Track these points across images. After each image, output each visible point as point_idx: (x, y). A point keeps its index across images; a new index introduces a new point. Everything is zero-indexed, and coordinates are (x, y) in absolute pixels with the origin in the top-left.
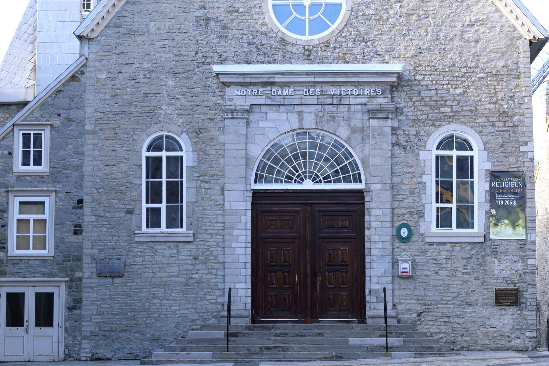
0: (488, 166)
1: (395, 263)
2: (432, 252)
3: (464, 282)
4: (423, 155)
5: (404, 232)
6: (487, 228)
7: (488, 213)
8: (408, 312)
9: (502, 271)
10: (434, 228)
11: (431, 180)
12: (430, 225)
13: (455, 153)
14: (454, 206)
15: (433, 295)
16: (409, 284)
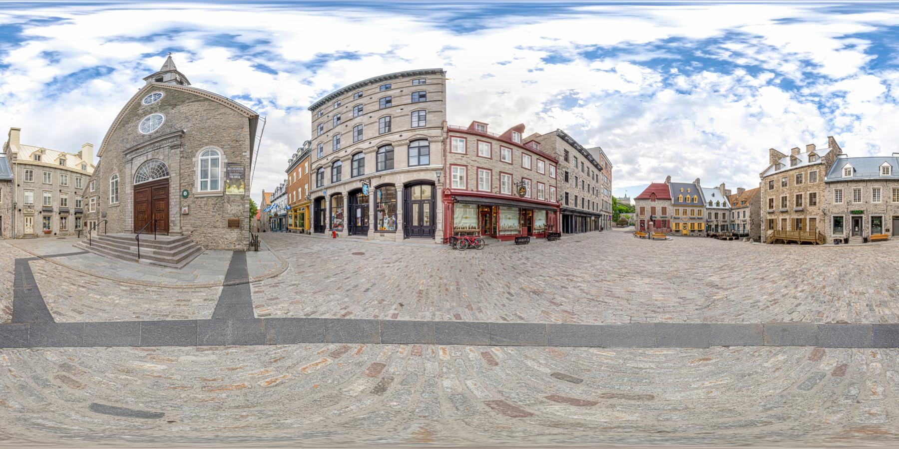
0: (226, 161)
1: (181, 209)
2: (198, 202)
3: (213, 216)
4: (194, 159)
5: (185, 194)
6: (225, 189)
7: (225, 182)
8: (187, 230)
9: (233, 210)
10: (199, 190)
11: (198, 170)
12: (198, 189)
13: (210, 157)
14: (209, 180)
15: (198, 223)
16: (188, 217)
